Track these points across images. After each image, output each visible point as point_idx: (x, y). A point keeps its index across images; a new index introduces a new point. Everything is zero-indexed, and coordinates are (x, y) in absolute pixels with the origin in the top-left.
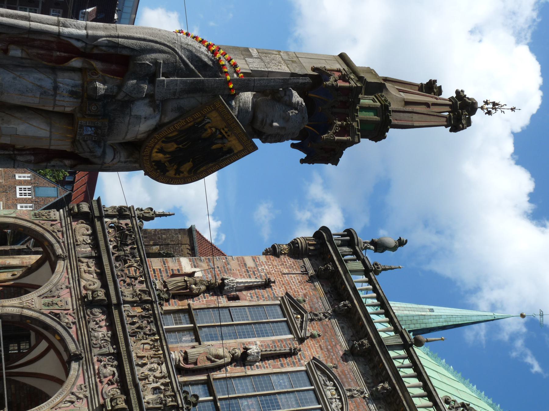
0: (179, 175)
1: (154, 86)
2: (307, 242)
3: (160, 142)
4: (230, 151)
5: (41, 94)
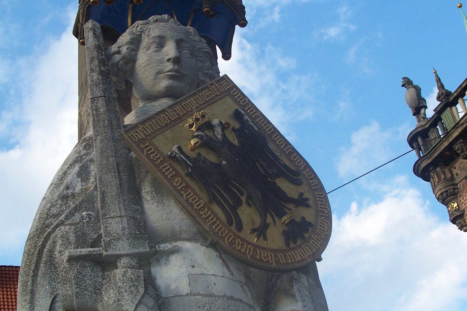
0: (307, 199)
1: (119, 257)
2: (436, 184)
3: (241, 235)
4: (237, 115)
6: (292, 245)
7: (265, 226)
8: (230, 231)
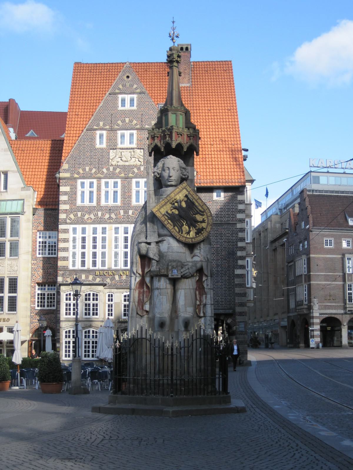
3: (182, 235)
4: (186, 196)
5: (160, 295)
6: (197, 236)
7: (190, 231)
8: (179, 234)
